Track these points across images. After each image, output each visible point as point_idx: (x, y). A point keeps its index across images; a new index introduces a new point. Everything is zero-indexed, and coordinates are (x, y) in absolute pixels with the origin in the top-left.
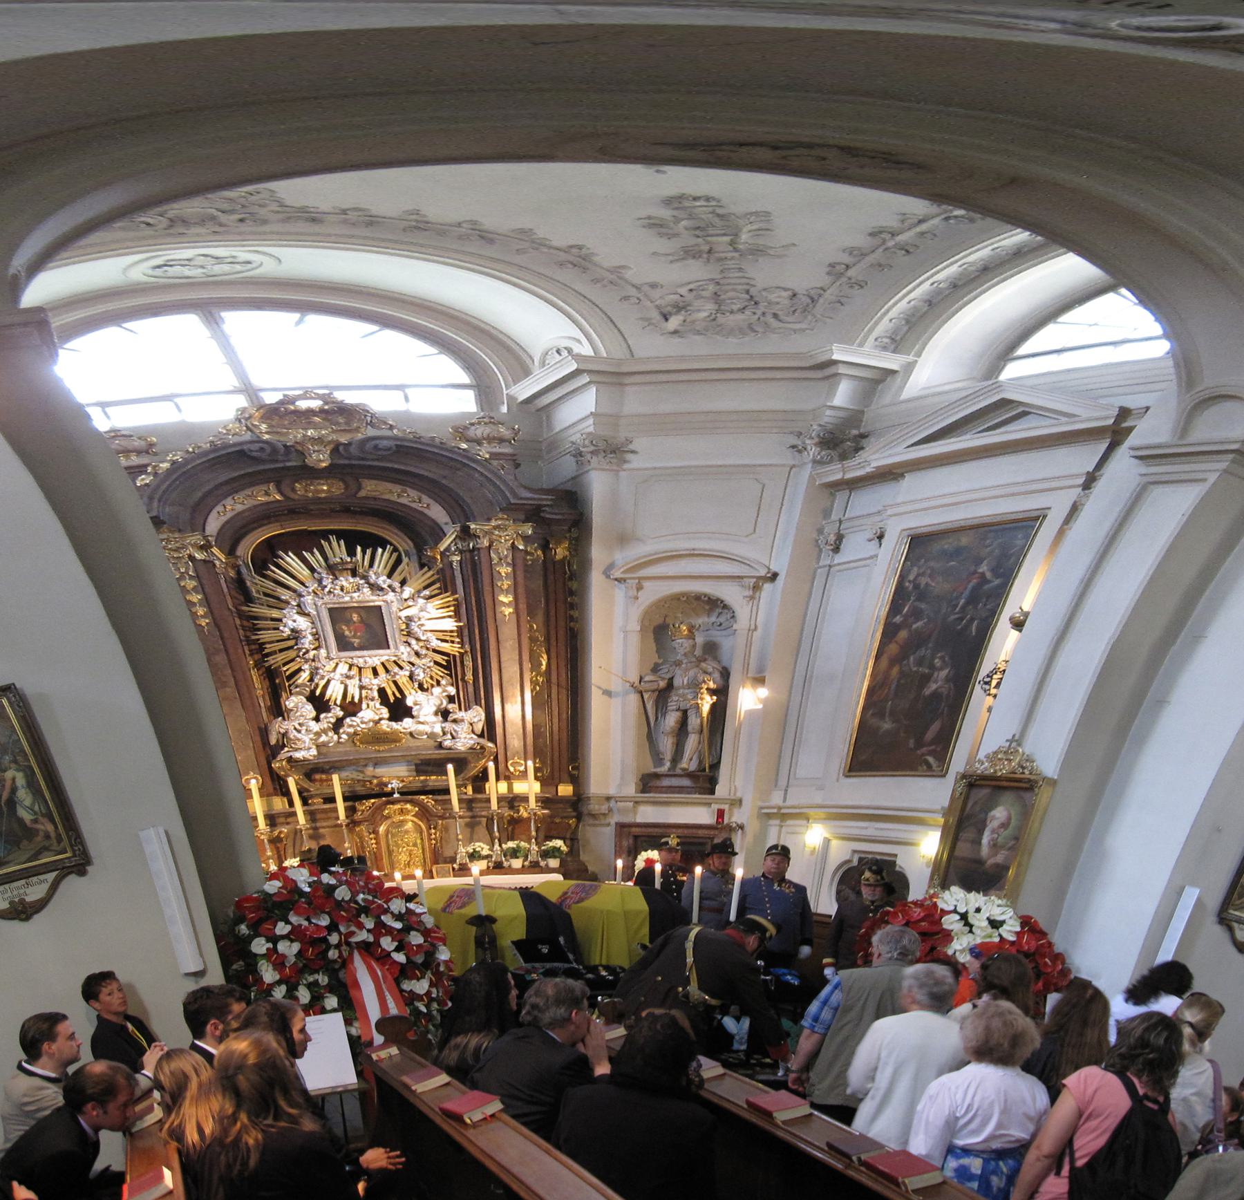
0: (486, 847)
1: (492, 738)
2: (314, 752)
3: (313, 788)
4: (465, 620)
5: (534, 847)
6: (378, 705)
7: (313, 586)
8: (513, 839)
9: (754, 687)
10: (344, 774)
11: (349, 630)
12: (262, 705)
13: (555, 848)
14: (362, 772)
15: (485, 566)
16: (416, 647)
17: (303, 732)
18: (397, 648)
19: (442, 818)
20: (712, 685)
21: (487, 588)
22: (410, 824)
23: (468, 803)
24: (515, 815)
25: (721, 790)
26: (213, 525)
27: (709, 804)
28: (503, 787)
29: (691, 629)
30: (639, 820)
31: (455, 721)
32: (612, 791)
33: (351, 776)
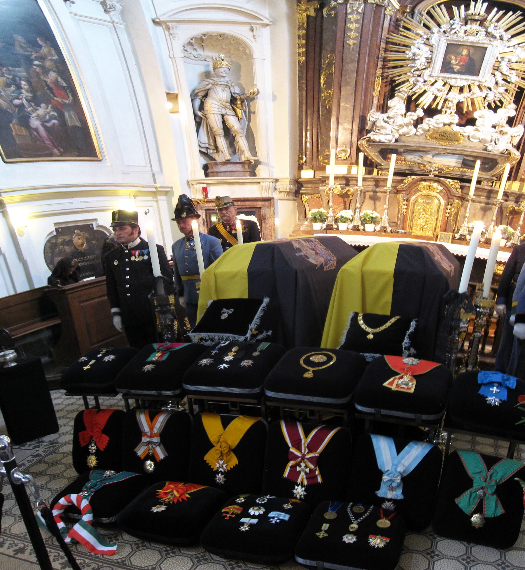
11: (456, 60)
14: (422, 157)
33: (414, 159)
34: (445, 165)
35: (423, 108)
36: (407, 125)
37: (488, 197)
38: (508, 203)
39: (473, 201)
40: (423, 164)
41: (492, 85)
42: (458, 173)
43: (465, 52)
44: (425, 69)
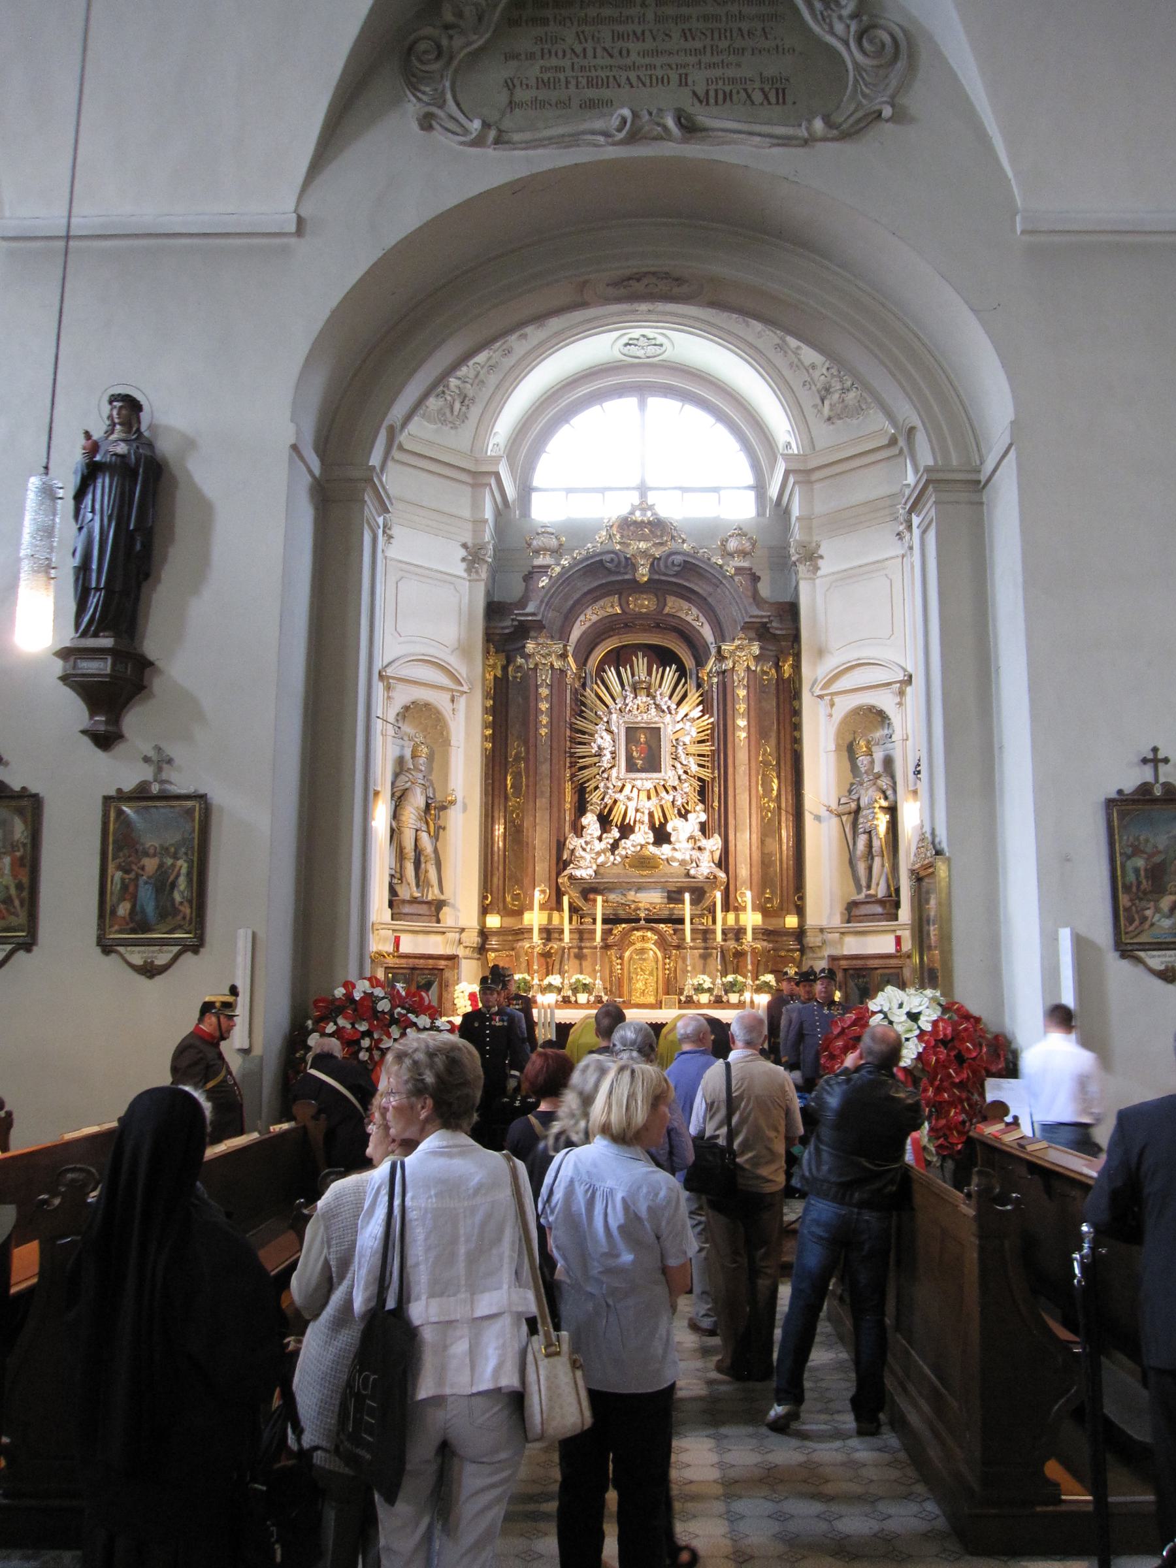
2: (591, 872)
3: (585, 908)
4: (716, 744)
5: (749, 981)
6: (647, 829)
10: (612, 897)
11: (637, 751)
12: (567, 818)
13: (766, 982)
17: (588, 850)
18: (666, 773)
19: (678, 947)
20: (884, 804)
21: (730, 712)
22: (651, 953)
24: (739, 948)
28: (731, 917)
31: (700, 849)
34: (651, 904)
35: (616, 826)
36: (603, 851)
37: (705, 940)
38: (728, 943)
39: (691, 948)
40: (628, 905)
41: (676, 783)
42: (665, 913)
44: (611, 768)
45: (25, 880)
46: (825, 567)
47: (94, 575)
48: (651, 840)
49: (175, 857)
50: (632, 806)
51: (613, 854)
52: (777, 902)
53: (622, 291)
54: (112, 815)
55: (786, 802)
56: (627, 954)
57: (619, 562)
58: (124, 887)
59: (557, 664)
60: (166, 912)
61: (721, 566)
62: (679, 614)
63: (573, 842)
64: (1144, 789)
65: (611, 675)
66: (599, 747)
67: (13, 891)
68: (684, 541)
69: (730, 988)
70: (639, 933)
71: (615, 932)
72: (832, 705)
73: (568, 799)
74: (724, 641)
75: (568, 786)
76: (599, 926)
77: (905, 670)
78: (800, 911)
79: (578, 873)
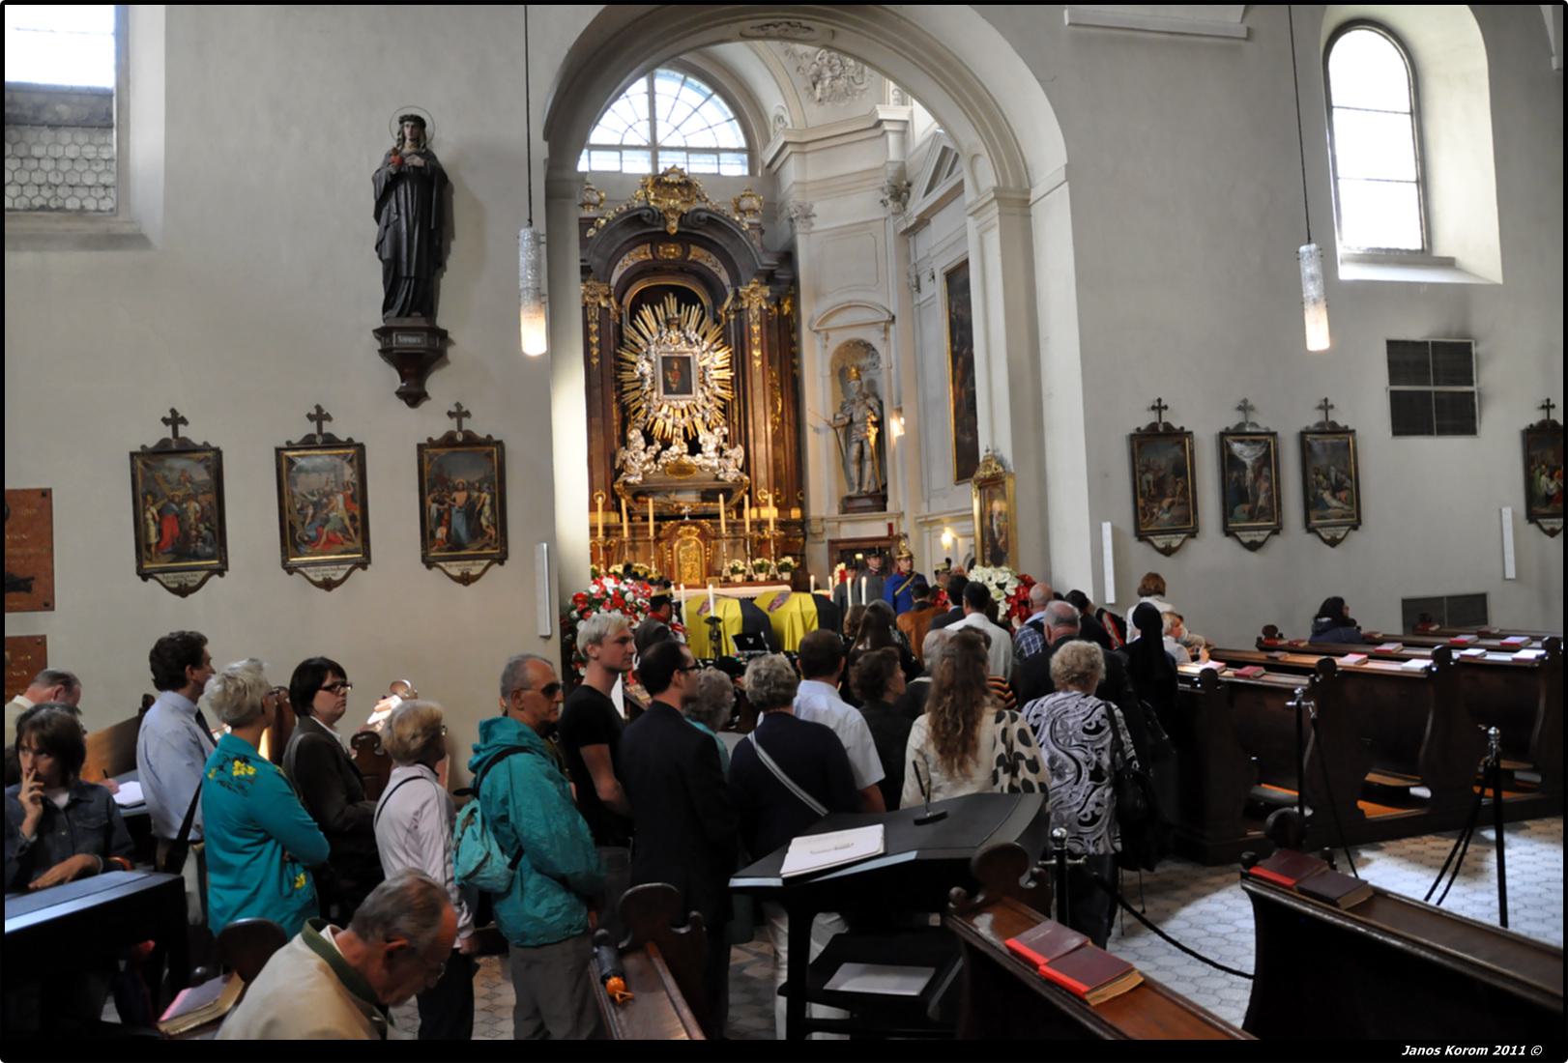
0: (742, 563)
1: (748, 474)
2: (640, 478)
3: (637, 508)
5: (773, 563)
7: (657, 337)
8: (759, 557)
9: (899, 417)
10: (657, 498)
15: (746, 323)
16: (707, 394)
19: (715, 538)
20: (874, 419)
23: (731, 526)
25: (890, 506)
26: (614, 280)
27: (884, 519)
28: (754, 511)
29: (858, 370)
30: (843, 537)
31: (726, 457)
32: (824, 514)
36: (648, 461)
41: (706, 404)
42: (701, 511)
43: (676, 367)
45: (357, 513)
46: (818, 224)
47: (404, 267)
48: (686, 451)
49: (480, 490)
50: (669, 422)
51: (656, 463)
52: (783, 498)
53: (762, 33)
54: (426, 458)
55: (789, 417)
56: (676, 546)
57: (654, 217)
58: (440, 515)
59: (603, 304)
60: (476, 531)
61: (738, 222)
62: (700, 261)
63: (624, 454)
64: (1153, 427)
65: (647, 313)
66: (642, 374)
67: (347, 522)
68: (707, 201)
69: (760, 568)
70: (687, 528)
71: (665, 527)
72: (827, 338)
73: (615, 417)
74: (740, 284)
75: (614, 406)
76: (651, 523)
77: (889, 312)
78: (802, 505)
79: (631, 480)
